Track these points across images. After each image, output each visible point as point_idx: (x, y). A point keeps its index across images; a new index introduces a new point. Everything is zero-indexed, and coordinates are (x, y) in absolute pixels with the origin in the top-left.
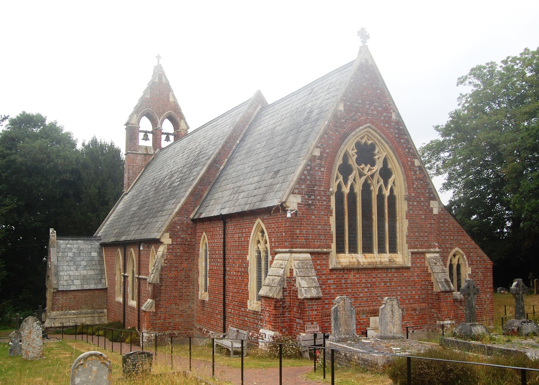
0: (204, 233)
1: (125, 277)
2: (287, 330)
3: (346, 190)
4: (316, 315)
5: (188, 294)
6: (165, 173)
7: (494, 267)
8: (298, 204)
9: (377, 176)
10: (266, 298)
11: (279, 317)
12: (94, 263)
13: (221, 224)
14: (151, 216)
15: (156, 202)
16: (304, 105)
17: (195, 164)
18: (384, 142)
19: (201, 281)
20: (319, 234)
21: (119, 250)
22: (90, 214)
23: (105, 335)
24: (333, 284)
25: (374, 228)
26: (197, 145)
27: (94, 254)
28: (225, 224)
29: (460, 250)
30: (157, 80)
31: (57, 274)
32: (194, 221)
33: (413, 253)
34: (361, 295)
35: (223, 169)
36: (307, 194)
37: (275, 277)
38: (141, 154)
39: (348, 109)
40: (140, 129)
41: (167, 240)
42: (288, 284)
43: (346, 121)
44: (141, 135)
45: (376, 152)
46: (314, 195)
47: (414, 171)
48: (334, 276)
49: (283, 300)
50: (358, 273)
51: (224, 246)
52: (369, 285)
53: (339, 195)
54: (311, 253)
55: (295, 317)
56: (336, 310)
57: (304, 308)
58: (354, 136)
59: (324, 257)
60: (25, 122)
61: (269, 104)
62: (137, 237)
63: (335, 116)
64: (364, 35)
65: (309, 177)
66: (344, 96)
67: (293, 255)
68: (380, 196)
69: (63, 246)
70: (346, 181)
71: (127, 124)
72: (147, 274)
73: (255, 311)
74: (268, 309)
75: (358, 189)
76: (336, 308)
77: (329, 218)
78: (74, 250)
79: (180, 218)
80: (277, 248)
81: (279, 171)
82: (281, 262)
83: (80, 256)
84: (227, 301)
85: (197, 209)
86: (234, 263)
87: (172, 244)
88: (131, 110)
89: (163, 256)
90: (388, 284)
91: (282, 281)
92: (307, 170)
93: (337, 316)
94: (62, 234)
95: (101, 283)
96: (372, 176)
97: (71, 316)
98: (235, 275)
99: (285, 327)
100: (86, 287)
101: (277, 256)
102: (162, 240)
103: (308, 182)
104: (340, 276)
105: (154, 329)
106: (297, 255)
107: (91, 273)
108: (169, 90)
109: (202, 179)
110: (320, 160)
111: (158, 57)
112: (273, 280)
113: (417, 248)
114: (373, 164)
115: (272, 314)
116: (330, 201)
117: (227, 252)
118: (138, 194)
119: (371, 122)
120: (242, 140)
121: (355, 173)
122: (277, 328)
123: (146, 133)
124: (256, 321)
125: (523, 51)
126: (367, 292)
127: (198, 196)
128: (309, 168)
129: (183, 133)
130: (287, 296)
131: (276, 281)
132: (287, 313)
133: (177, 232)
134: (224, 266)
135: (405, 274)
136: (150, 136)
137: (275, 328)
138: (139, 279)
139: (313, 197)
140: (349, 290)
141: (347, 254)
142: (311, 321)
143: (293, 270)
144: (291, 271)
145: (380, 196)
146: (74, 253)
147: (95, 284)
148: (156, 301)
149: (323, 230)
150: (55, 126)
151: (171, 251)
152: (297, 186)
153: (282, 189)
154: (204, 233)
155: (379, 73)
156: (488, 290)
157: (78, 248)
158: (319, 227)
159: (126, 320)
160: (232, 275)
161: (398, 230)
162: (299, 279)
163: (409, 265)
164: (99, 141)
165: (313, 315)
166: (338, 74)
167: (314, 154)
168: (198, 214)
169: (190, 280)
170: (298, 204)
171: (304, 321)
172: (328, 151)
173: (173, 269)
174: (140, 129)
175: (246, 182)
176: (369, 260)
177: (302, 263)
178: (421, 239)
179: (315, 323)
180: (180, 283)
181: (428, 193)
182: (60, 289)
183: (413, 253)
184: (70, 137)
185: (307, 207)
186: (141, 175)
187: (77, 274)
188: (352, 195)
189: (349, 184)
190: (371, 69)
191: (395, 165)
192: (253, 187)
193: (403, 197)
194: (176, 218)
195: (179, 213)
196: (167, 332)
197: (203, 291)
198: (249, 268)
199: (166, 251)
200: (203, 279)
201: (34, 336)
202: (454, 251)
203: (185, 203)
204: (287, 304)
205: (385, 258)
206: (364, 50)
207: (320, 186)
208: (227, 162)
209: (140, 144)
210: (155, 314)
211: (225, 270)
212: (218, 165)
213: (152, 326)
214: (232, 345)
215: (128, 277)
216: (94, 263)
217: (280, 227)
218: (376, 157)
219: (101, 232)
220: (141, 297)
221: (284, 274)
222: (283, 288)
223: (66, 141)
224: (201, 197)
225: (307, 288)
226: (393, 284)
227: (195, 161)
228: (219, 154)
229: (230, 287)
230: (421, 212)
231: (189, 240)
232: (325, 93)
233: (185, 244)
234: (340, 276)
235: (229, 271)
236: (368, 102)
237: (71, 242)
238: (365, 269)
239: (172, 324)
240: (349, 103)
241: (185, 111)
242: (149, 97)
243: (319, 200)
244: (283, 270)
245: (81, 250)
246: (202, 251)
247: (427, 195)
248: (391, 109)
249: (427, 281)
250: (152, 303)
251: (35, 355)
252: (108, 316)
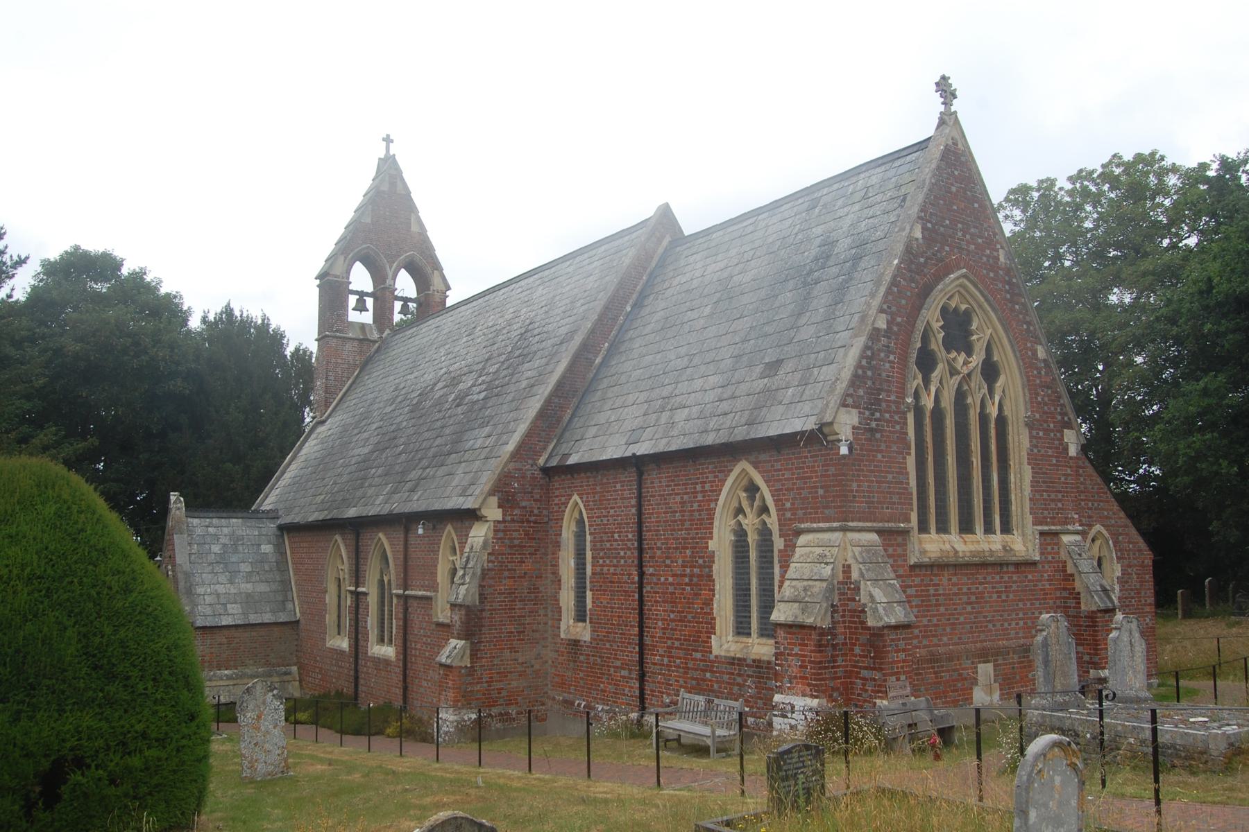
0: (576, 497)
1: (357, 596)
2: (841, 694)
3: (928, 403)
4: (904, 661)
5: (535, 627)
6: (428, 377)
7: (1155, 562)
8: (854, 428)
9: (977, 379)
10: (790, 627)
11: (826, 668)
12: (267, 568)
13: (630, 476)
14: (425, 462)
15: (426, 435)
16: (801, 231)
17: (520, 353)
18: (988, 308)
19: (567, 598)
20: (890, 493)
21: (338, 538)
22: (229, 465)
23: (315, 721)
24: (917, 596)
25: (975, 482)
26: (508, 316)
27: (267, 548)
28: (640, 474)
29: (1105, 532)
30: (385, 188)
31: (190, 592)
32: (546, 471)
33: (1042, 534)
34: (962, 619)
35: (601, 364)
36: (867, 409)
37: (810, 583)
38: (354, 339)
39: (931, 236)
40: (351, 287)
41: (493, 513)
42: (844, 594)
43: (926, 262)
44: (352, 300)
45: (974, 326)
46: (880, 411)
47: (1037, 369)
48: (917, 580)
49: (831, 631)
50: (955, 574)
51: (640, 523)
52: (973, 598)
53: (919, 411)
54: (879, 532)
55: (860, 668)
56: (1045, 644)
57: (884, 646)
58: (942, 290)
59: (900, 539)
60: (79, 268)
61: (686, 233)
62: (398, 505)
63: (908, 249)
64: (945, 89)
65: (869, 373)
66: (922, 211)
67: (850, 535)
68: (984, 418)
69: (199, 531)
70: (927, 382)
71: (321, 277)
72: (434, 587)
73: (734, 658)
74: (796, 650)
75: (948, 402)
76: (1046, 638)
77: (904, 458)
78: (223, 540)
79: (519, 465)
80: (802, 521)
81: (779, 362)
82: (819, 550)
83: (236, 551)
84: (648, 640)
85: (551, 447)
86: (667, 558)
87: (504, 521)
88: (328, 248)
89: (485, 543)
90: (1004, 597)
91: (830, 590)
92: (867, 357)
93: (1047, 655)
94: (196, 505)
95: (284, 610)
96: (969, 375)
97: (222, 683)
98: (671, 584)
99: (838, 689)
100: (253, 619)
101: (803, 539)
102: (484, 512)
103: (869, 383)
104: (927, 581)
105: (468, 706)
106: (856, 536)
107: (263, 588)
108: (411, 208)
109: (559, 385)
110: (889, 338)
111: (388, 140)
112: (805, 590)
113: (1047, 524)
115: (810, 662)
116: (905, 424)
117: (646, 535)
118: (359, 421)
120: (638, 305)
122: (824, 692)
123: (362, 295)
124: (739, 680)
125: (1146, 152)
126: (970, 613)
127: (555, 418)
128: (869, 353)
129: (437, 298)
130: (838, 622)
131: (816, 590)
132: (840, 658)
133: (514, 494)
134: (640, 566)
135: (1030, 577)
136: (370, 302)
137: (816, 692)
138: (407, 597)
139: (877, 415)
140: (942, 609)
141: (934, 535)
142: (898, 673)
143: (849, 566)
144: (847, 569)
145: (984, 418)
146: (224, 545)
147: (273, 612)
148: (472, 643)
149: (896, 483)
150: (142, 279)
151: (501, 535)
152: (851, 391)
153: (804, 397)
154: (576, 497)
155: (977, 167)
156: (1147, 609)
157: (231, 536)
158: (890, 477)
159: (361, 688)
160: (664, 584)
161: (1013, 486)
162: (867, 587)
163: (1037, 558)
164: (237, 313)
165: (899, 662)
166: (883, 168)
167: (876, 326)
168: (558, 458)
169: (539, 598)
170: (854, 428)
171: (884, 675)
172: (899, 319)
173: (506, 574)
174: (351, 287)
175: (683, 387)
176: (972, 547)
177: (868, 552)
178: (1053, 505)
179: (903, 677)
180: (519, 605)
181: (1061, 414)
182: (199, 623)
183: (1042, 534)
184: (177, 305)
185: (868, 435)
186: (353, 382)
187: (233, 591)
188: (938, 413)
189: (933, 390)
190: (963, 159)
191: (1007, 358)
192: (711, 396)
193: (1021, 420)
194: (511, 466)
195: (516, 455)
196: (494, 711)
197: (571, 621)
198: (715, 567)
199: (491, 535)
200: (572, 595)
201: (266, 724)
203: (529, 435)
204: (840, 639)
206: (948, 120)
207: (889, 392)
208: (608, 350)
209: (350, 319)
210: (471, 671)
211: (642, 574)
212: (591, 356)
213: (464, 699)
214: (713, 732)
215: (365, 594)
216: (267, 568)
217: (811, 477)
218: (974, 337)
219: (270, 500)
220: (410, 637)
221: (833, 575)
222: (833, 606)
223: (167, 310)
224: (558, 422)
225: (884, 604)
226: (1011, 596)
227: (515, 348)
228: (592, 331)
229: (658, 612)
230: (1050, 452)
231: (536, 511)
232: (857, 207)
233: (528, 522)
234: (927, 581)
235: (651, 575)
236: (960, 226)
237: (215, 521)
238: (967, 565)
239: (504, 693)
240: (929, 225)
241: (442, 254)
242: (368, 220)
243: (888, 421)
244: (830, 567)
245: (238, 540)
246: (568, 533)
247: (1059, 418)
248: (997, 242)
249: (1065, 589)
250: (463, 648)
251: (271, 768)
252: (300, 681)
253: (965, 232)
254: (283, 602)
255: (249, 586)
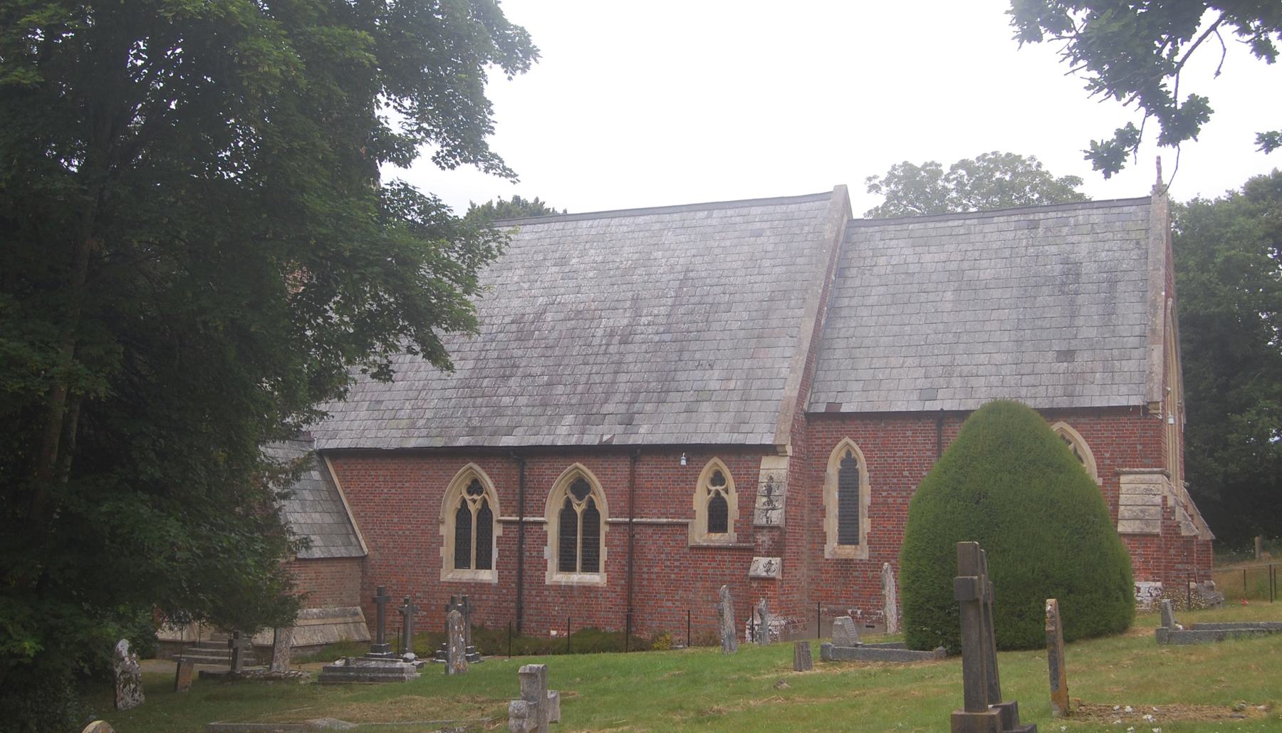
74: (1139, 551)
95: (351, 544)
97: (314, 622)
101: (1123, 479)
107: (328, 519)
144: (1165, 499)
187: (309, 521)
254: (348, 534)
255: (317, 515)
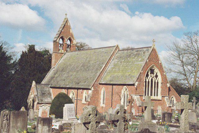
33: (162, 97)
41: (92, 89)
54: (140, 96)
75: (150, 80)
114: (154, 74)
119: (155, 64)
121: (150, 76)
145: (155, 82)
183: (162, 97)
188: (149, 82)
191: (159, 74)
202: (172, 96)
205: (156, 98)
211: (112, 98)
253: (154, 59)
